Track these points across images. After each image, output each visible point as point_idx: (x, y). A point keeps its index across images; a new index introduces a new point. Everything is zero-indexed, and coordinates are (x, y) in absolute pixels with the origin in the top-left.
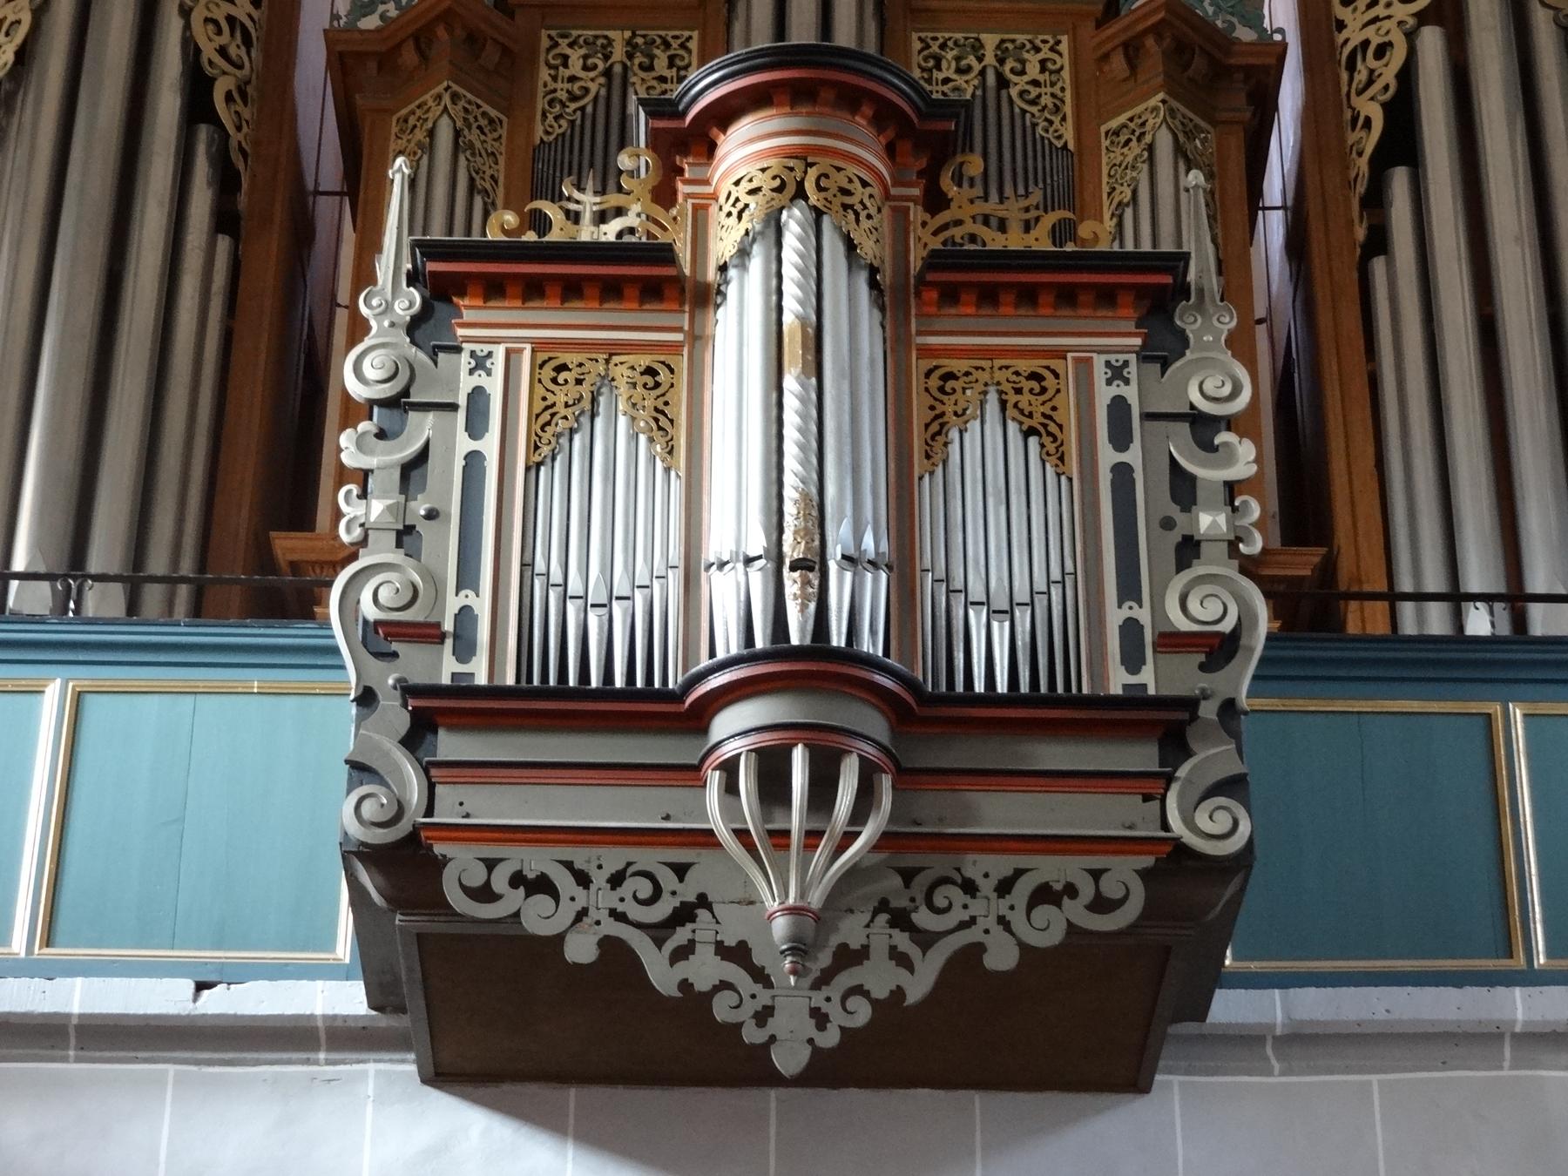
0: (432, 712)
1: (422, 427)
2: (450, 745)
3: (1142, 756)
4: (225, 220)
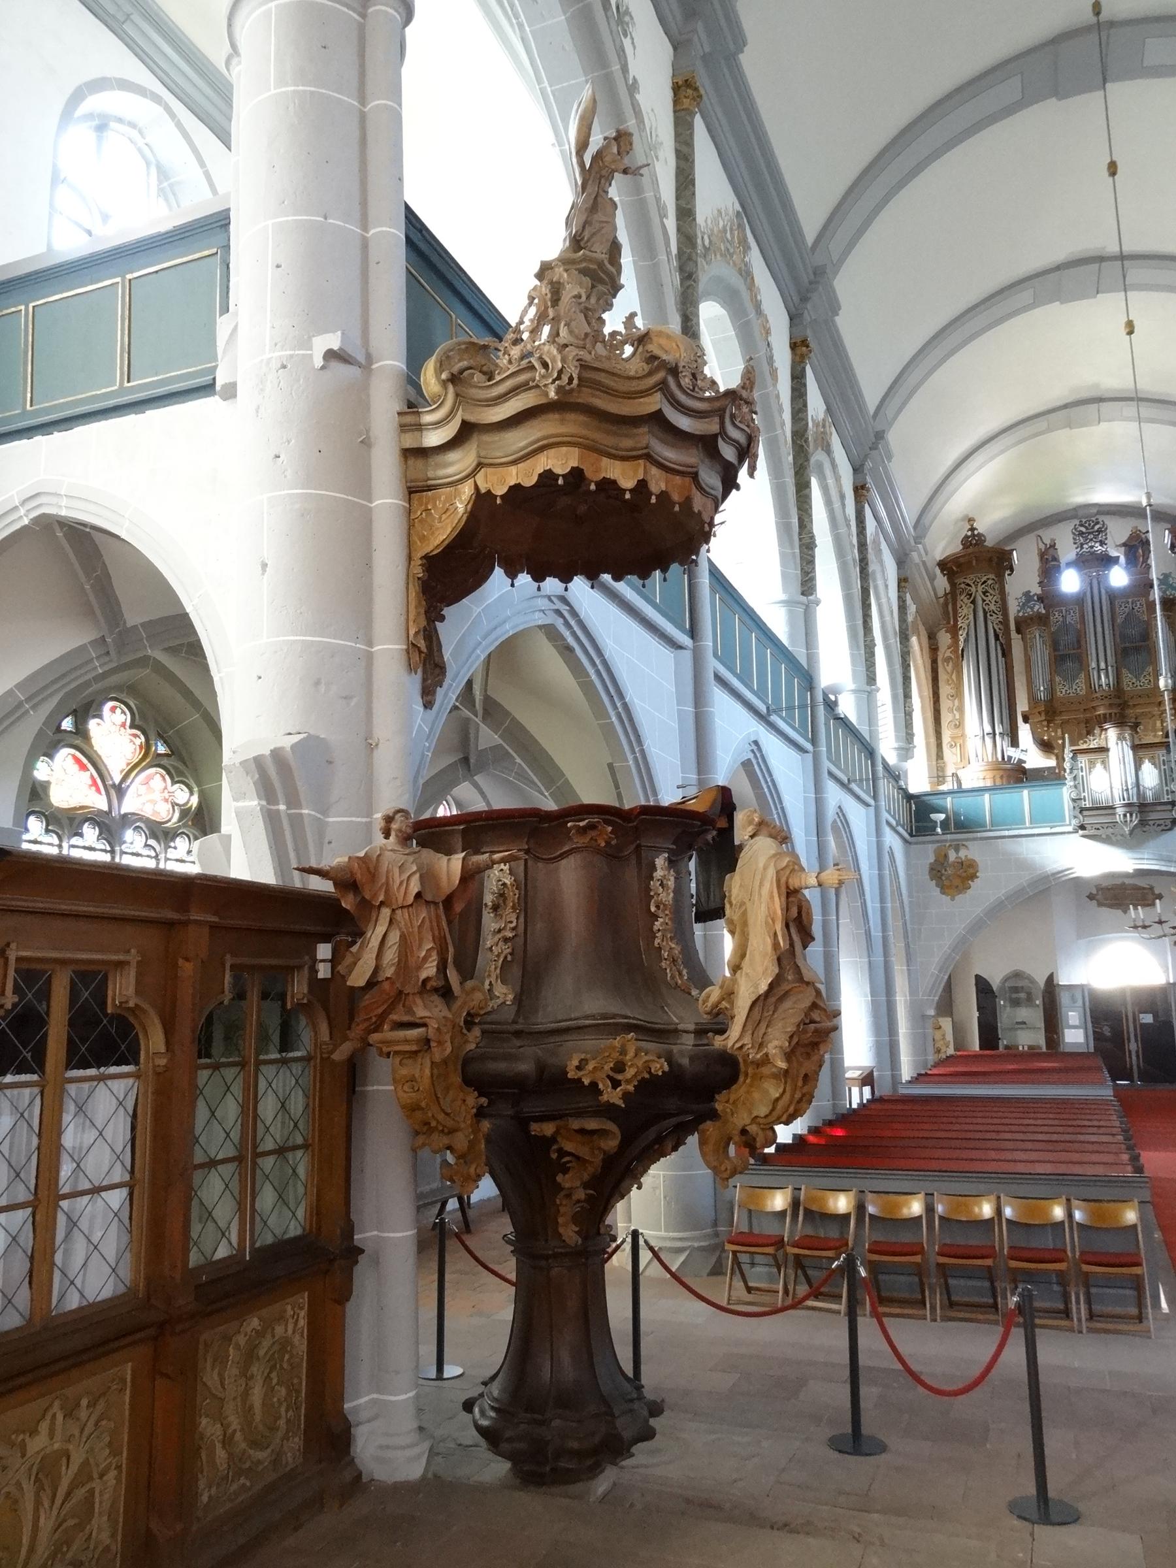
0: (1082, 810)
1: (1075, 772)
2: (1085, 813)
3: (1169, 807)
4: (1004, 655)
